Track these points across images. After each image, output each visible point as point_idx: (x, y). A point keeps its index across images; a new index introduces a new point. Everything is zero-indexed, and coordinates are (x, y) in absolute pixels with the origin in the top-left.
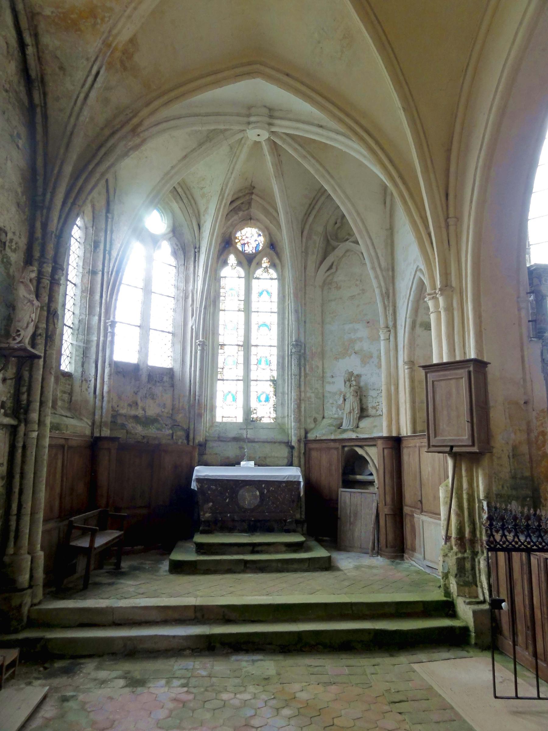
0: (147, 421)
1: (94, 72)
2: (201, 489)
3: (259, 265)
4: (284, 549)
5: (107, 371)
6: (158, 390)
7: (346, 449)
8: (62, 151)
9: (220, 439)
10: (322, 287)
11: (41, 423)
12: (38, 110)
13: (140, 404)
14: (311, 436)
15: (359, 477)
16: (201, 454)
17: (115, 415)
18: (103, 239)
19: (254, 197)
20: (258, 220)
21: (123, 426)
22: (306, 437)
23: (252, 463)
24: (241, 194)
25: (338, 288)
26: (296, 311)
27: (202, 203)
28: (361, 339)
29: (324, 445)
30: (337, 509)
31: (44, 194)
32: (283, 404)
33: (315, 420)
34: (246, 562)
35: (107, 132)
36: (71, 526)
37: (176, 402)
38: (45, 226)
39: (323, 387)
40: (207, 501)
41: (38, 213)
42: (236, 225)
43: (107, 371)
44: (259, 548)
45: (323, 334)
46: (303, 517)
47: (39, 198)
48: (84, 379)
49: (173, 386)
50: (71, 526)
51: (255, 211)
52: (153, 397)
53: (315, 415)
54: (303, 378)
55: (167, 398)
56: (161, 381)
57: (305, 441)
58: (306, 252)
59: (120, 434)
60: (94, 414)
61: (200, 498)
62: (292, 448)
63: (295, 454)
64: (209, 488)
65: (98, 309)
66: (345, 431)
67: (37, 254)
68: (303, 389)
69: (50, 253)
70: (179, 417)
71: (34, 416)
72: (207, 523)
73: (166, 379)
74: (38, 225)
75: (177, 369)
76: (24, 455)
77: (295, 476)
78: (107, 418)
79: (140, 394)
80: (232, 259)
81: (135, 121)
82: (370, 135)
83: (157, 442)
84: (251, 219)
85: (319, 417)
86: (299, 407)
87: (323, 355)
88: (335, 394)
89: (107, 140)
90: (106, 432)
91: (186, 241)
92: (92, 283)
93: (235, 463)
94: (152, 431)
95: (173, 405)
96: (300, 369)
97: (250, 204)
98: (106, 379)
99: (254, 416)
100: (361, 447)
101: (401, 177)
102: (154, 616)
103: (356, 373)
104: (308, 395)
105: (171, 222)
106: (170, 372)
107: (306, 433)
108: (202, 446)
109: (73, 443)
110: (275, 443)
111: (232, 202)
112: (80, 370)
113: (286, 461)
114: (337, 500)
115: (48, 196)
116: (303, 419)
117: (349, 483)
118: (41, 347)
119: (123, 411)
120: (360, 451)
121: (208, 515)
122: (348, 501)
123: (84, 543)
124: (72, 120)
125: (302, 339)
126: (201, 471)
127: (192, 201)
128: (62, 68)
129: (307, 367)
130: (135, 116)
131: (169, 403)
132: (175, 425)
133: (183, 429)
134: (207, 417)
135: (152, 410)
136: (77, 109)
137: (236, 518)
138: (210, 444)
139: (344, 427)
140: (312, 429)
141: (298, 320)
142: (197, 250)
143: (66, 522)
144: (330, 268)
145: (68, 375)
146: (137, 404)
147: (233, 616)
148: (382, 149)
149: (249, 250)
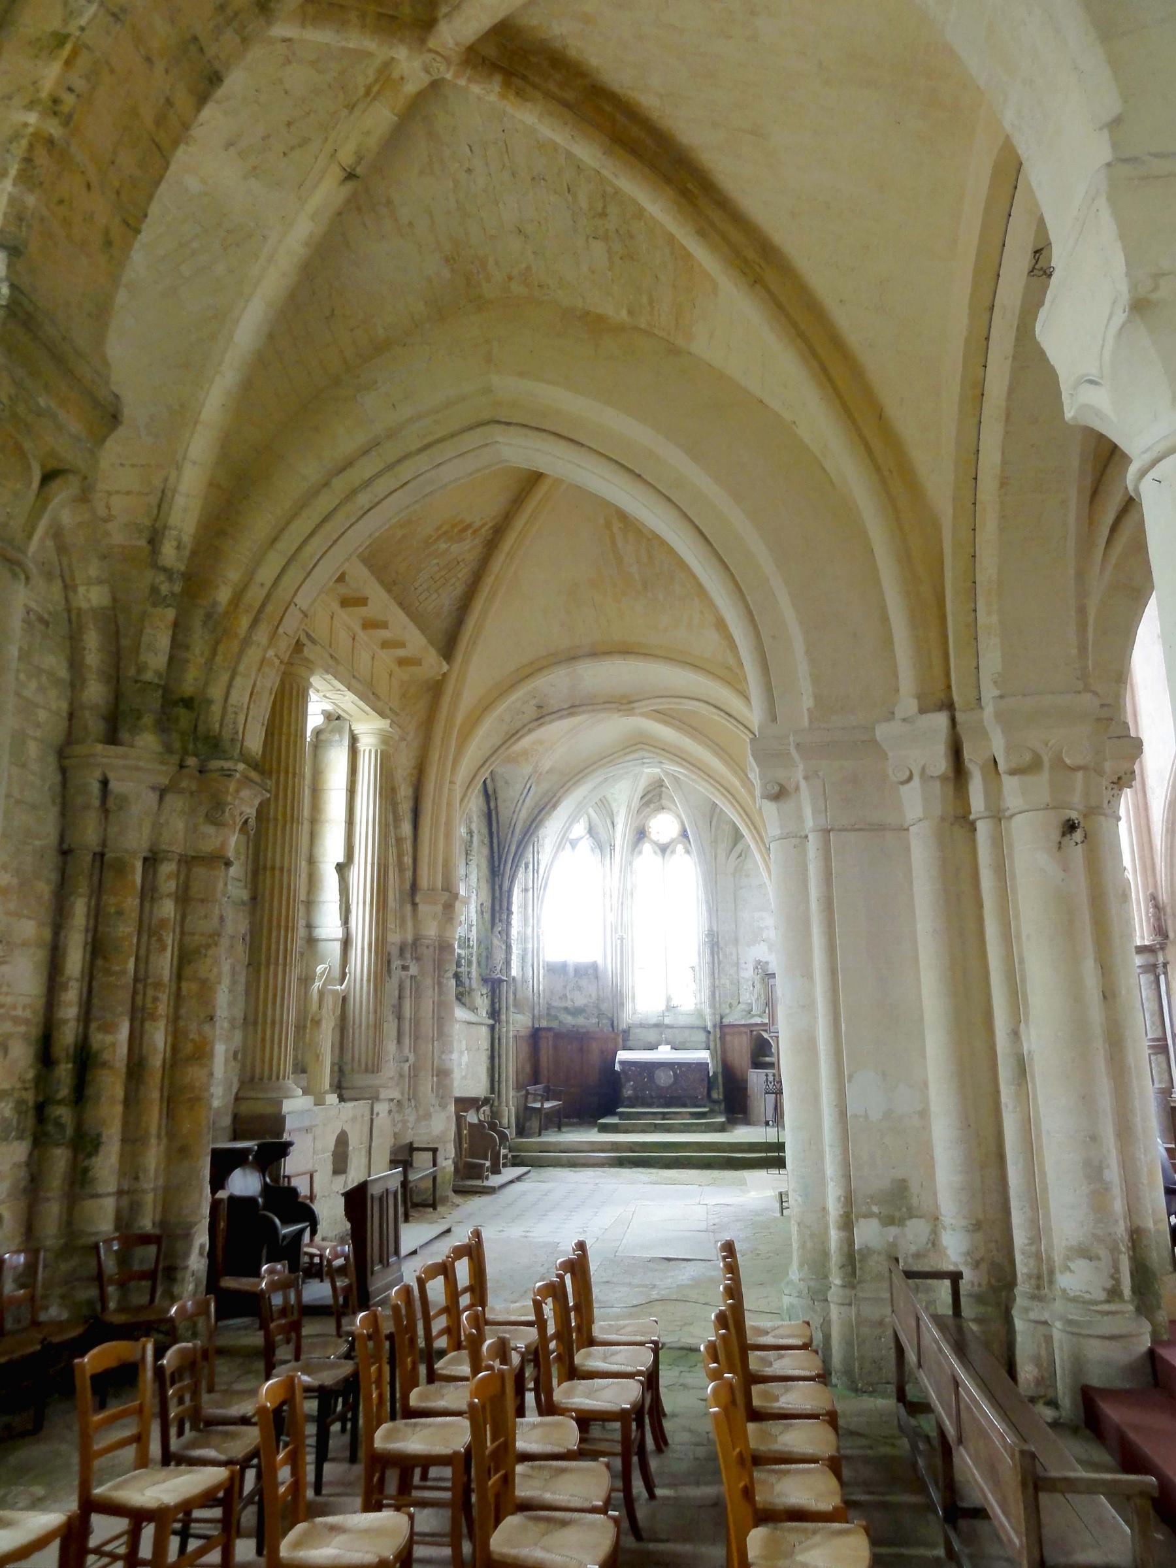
0: (576, 1012)
1: (528, 786)
2: (623, 1071)
3: (673, 852)
4: (688, 1116)
5: (541, 972)
6: (583, 983)
7: (755, 1033)
8: (509, 836)
9: (641, 1026)
10: (734, 875)
11: (507, 1022)
12: (494, 812)
13: (569, 997)
14: (726, 1021)
15: (767, 1059)
16: (625, 1040)
17: (549, 1007)
18: (531, 860)
19: (663, 789)
20: (670, 809)
21: (556, 1018)
22: (721, 1022)
23: (669, 1047)
24: (651, 788)
25: (747, 876)
26: (707, 902)
27: (614, 806)
28: (767, 928)
29: (736, 1030)
30: (746, 1089)
31: (499, 866)
32: (700, 991)
33: (731, 1006)
34: (656, 1125)
35: (536, 812)
36: (528, 1093)
37: (601, 993)
38: (501, 887)
39: (738, 972)
40: (629, 1081)
41: (497, 879)
42: (649, 816)
43: (541, 972)
44: (667, 1116)
45: (736, 921)
46: (721, 1097)
47: (496, 869)
48: (524, 981)
49: (597, 978)
50: (528, 1093)
51: (664, 802)
52: (580, 989)
53: (729, 1001)
54: (716, 965)
55: (592, 990)
56: (586, 974)
57: (722, 1027)
58: (715, 842)
59: (554, 1024)
60: (534, 1010)
61: (622, 1076)
62: (709, 1032)
63: (712, 1037)
64: (630, 1070)
65: (531, 921)
66: (754, 1016)
67: (497, 908)
68: (716, 976)
69: (505, 904)
70: (604, 1007)
71: (503, 1017)
72: (629, 1098)
73: (590, 971)
74: (497, 887)
75: (600, 962)
76: (499, 1044)
77: (704, 1058)
78: (544, 1012)
79: (569, 988)
80: (647, 847)
81: (555, 800)
82: (729, 792)
83: (584, 1030)
84: (663, 808)
85: (735, 1003)
86: (713, 994)
87: (736, 942)
88: (748, 980)
89: (536, 817)
90: (544, 1024)
91: (602, 840)
92: (525, 899)
93: (652, 1047)
94: (580, 1021)
95: (598, 995)
96: (713, 957)
97: (660, 795)
98: (541, 979)
99: (674, 1003)
100: (766, 1031)
101: (753, 824)
102: (585, 1147)
103: (764, 960)
104: (723, 981)
105: (587, 824)
106: (594, 966)
107: (722, 1018)
108: (626, 1032)
109: (522, 1034)
110: (693, 1028)
111: (642, 798)
112: (521, 973)
113: (704, 1045)
114: (746, 1081)
115: (502, 868)
116: (717, 1005)
117: (757, 1065)
118: (504, 971)
119: (555, 1004)
120: (765, 1035)
121: (630, 1092)
122: (755, 1081)
123: (538, 1105)
124: (515, 817)
125: (715, 929)
126: (622, 1055)
127: (607, 805)
128: (506, 783)
129: (721, 955)
130: (555, 796)
131: (594, 995)
132: (600, 1015)
133: (607, 1018)
134: (629, 1007)
135: (580, 1000)
136: (518, 809)
137: (654, 1094)
138: (633, 1031)
139: (754, 1012)
140: (727, 1014)
141: (709, 911)
142: (612, 847)
143: (524, 1092)
144: (740, 856)
145: (514, 978)
146: (565, 996)
147: (637, 1149)
148: (737, 801)
149: (664, 839)
